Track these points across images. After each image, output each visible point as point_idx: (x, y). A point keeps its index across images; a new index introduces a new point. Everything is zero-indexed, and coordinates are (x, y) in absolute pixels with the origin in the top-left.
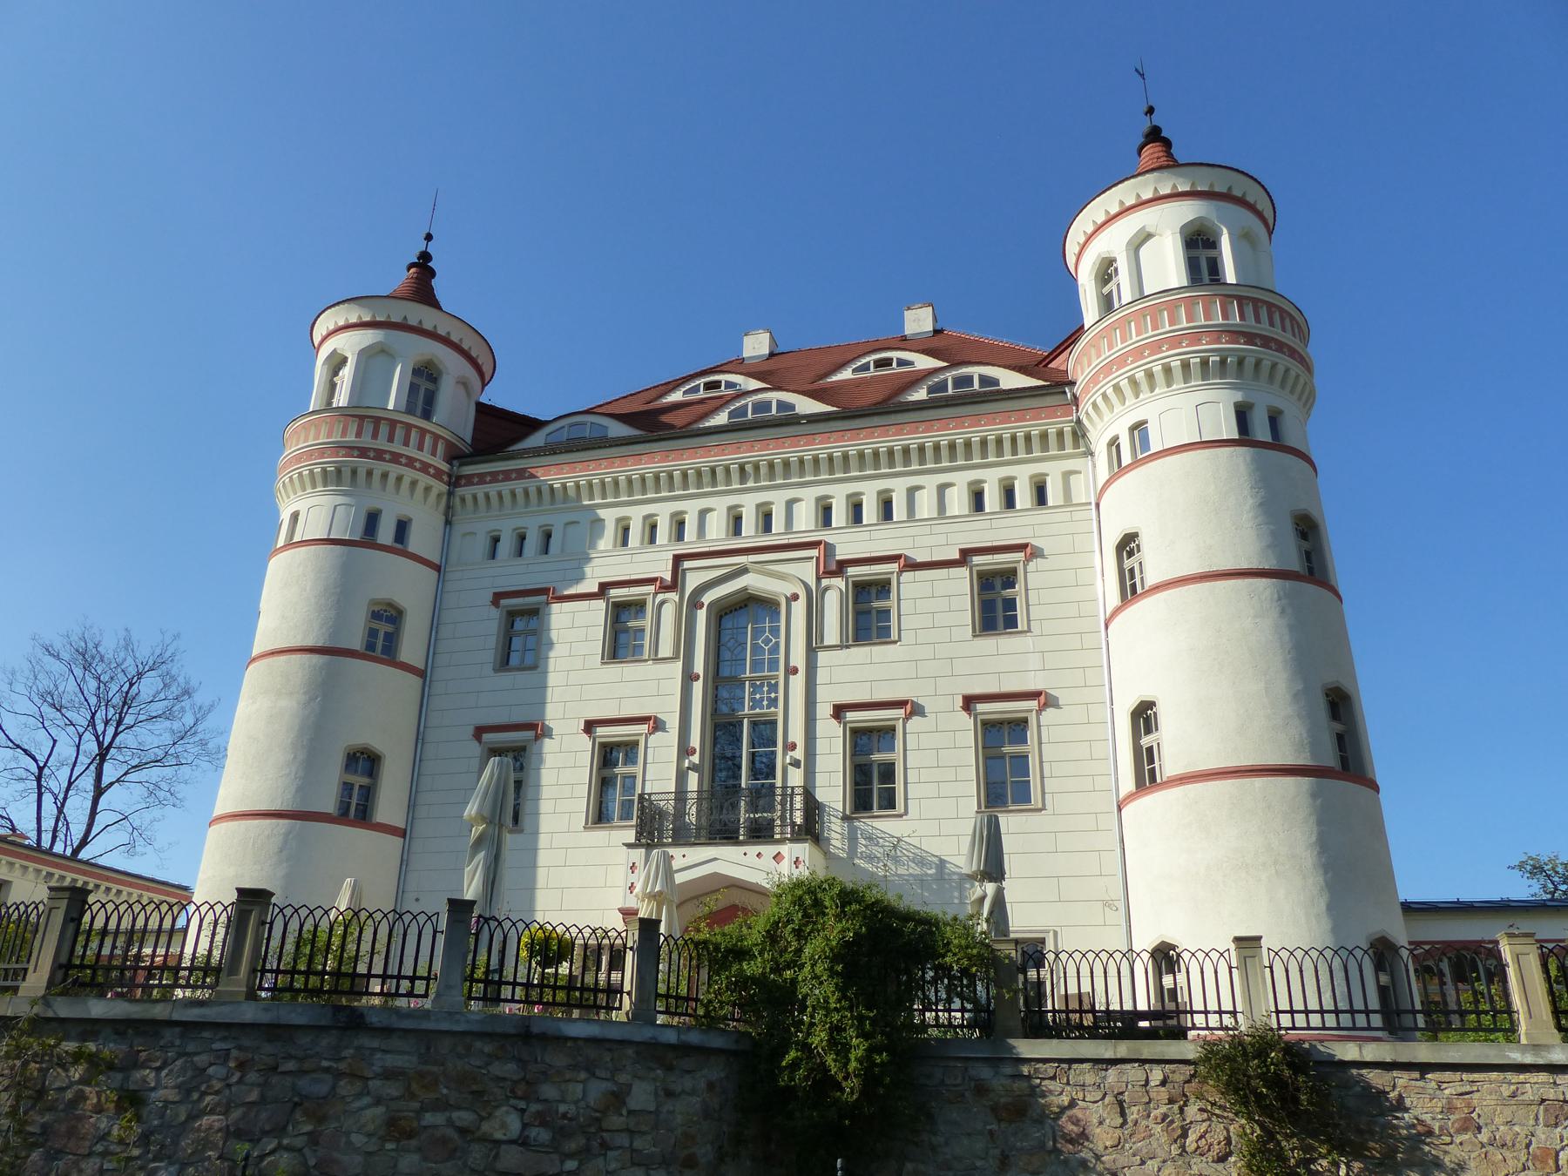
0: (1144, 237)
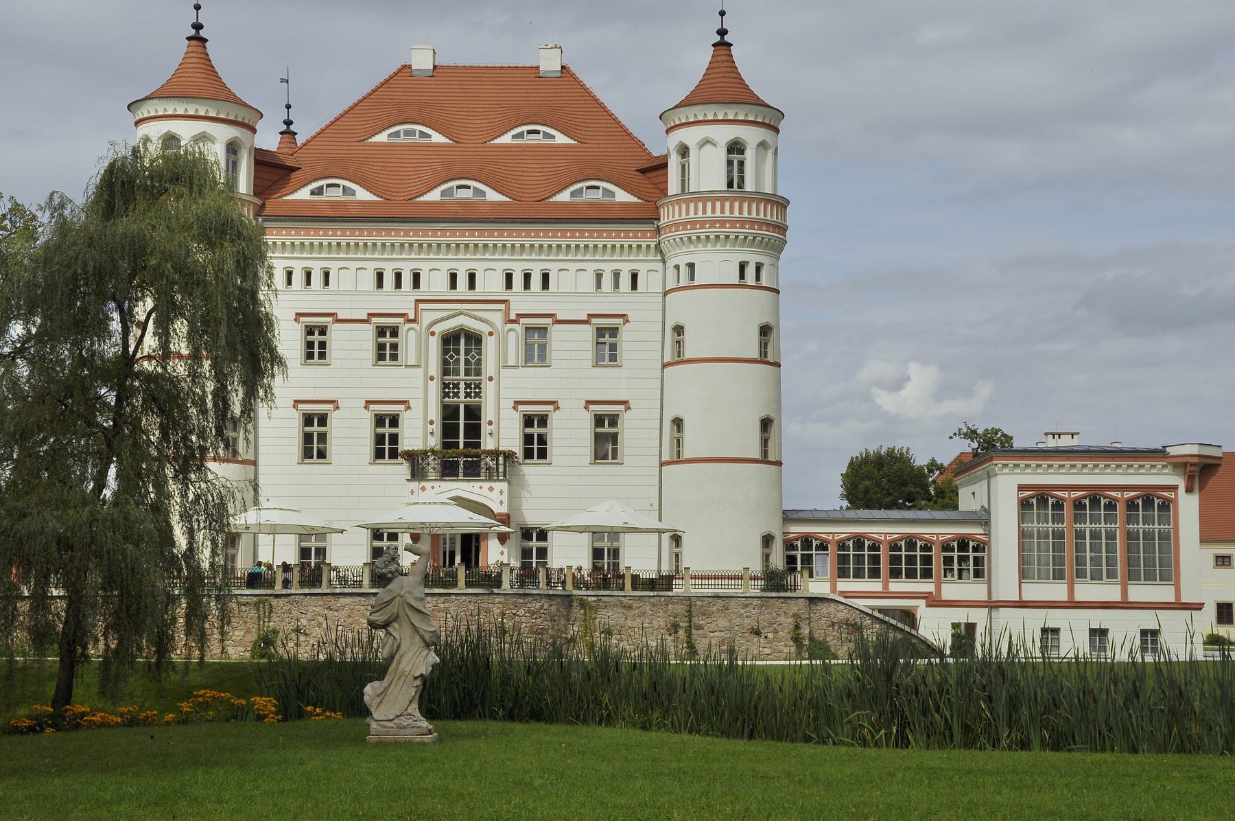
0: (707, 142)
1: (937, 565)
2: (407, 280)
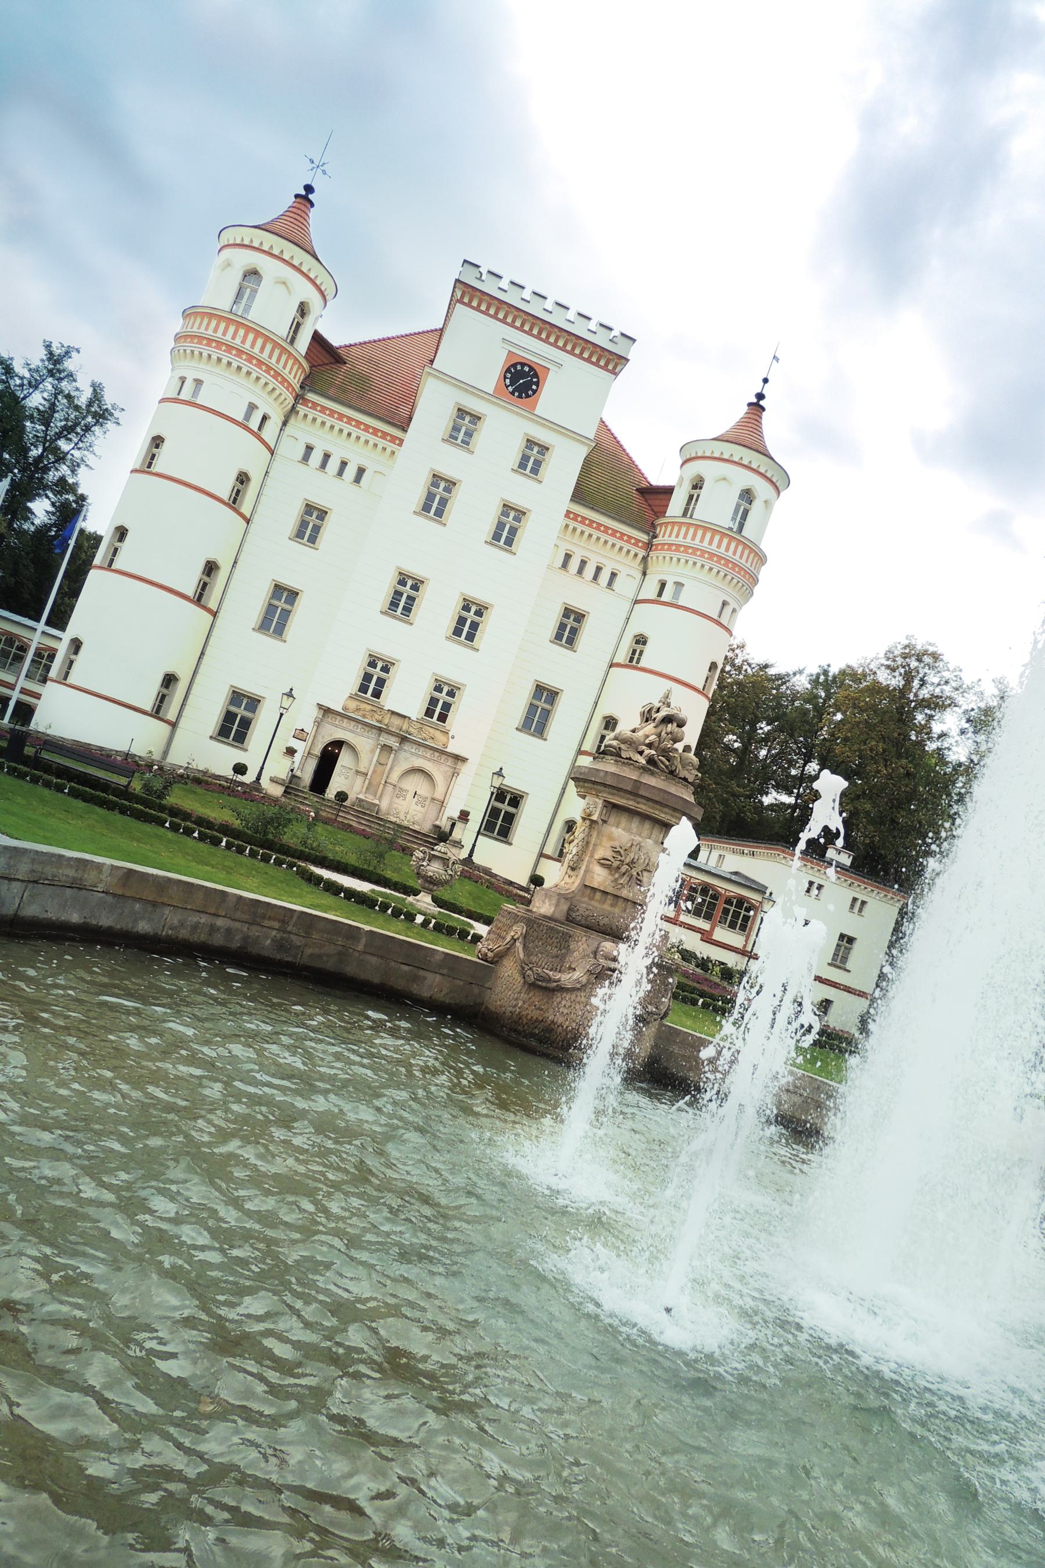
1: (718, 913)
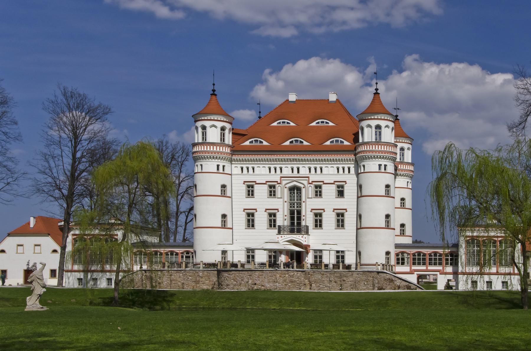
2: (278, 170)
